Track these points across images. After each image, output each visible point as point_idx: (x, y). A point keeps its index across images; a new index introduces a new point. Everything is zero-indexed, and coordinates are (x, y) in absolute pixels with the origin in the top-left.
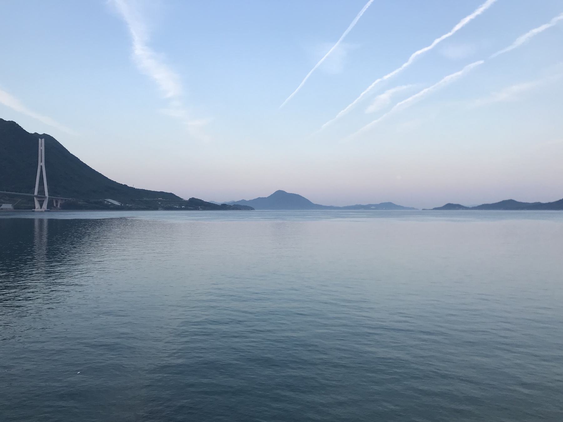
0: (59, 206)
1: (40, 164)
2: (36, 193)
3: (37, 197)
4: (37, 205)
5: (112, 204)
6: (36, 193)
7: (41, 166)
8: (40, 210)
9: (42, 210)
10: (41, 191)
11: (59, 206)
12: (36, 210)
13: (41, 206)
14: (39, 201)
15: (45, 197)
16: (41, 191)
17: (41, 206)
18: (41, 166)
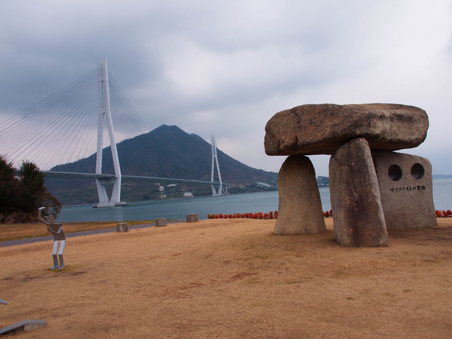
0: (226, 191)
1: (213, 156)
2: (212, 181)
3: (214, 184)
4: (214, 191)
5: (264, 186)
6: (212, 181)
7: (215, 158)
8: (216, 195)
9: (218, 195)
10: (216, 179)
11: (226, 191)
12: (213, 195)
13: (217, 191)
14: (215, 188)
15: (220, 184)
16: (216, 179)
17: (217, 191)
18: (215, 158)
